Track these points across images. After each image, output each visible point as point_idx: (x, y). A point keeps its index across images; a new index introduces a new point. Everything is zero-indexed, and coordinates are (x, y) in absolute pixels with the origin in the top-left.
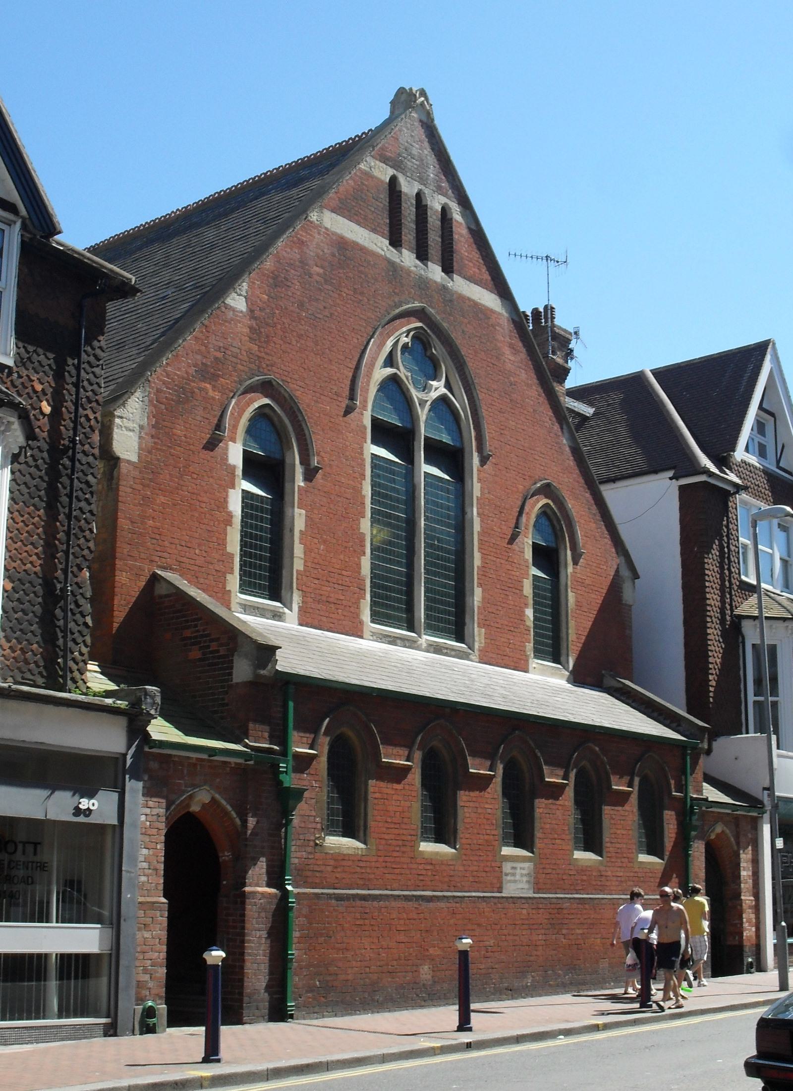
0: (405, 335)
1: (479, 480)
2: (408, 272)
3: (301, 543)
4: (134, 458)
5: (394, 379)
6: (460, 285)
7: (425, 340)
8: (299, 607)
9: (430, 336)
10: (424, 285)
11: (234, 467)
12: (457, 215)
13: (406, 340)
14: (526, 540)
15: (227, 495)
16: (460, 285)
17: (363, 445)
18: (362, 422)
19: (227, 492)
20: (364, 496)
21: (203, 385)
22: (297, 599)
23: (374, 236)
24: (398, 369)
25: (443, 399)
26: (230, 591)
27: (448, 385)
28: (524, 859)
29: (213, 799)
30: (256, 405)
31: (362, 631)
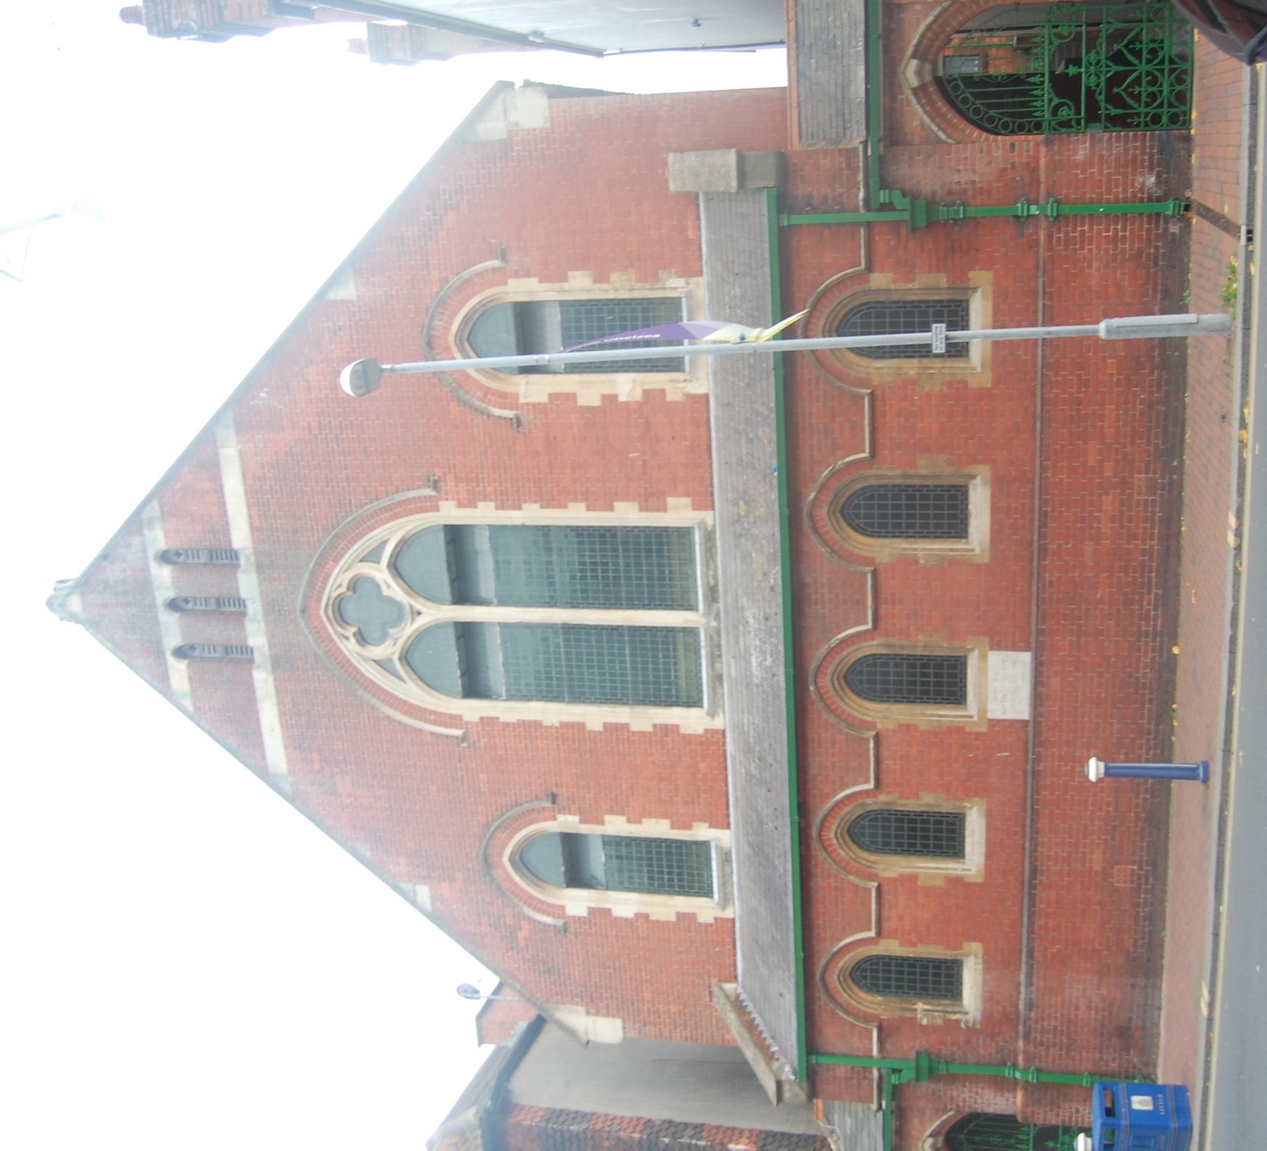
0: (345, 641)
1: (472, 504)
2: (271, 636)
3: (640, 823)
4: (618, 1022)
5: (405, 658)
6: (241, 537)
7: (337, 601)
8: (711, 826)
9: (329, 599)
10: (273, 609)
11: (592, 911)
12: (158, 539)
13: (353, 640)
14: (522, 400)
15: (620, 918)
16: (241, 537)
17: (503, 723)
18: (477, 723)
19: (616, 919)
20: (561, 723)
21: (522, 943)
22: (702, 832)
23: (260, 693)
24: (393, 653)
25: (394, 567)
26: (716, 919)
27: (372, 556)
28: (983, 671)
29: (930, 1136)
30: (517, 878)
31: (717, 731)
